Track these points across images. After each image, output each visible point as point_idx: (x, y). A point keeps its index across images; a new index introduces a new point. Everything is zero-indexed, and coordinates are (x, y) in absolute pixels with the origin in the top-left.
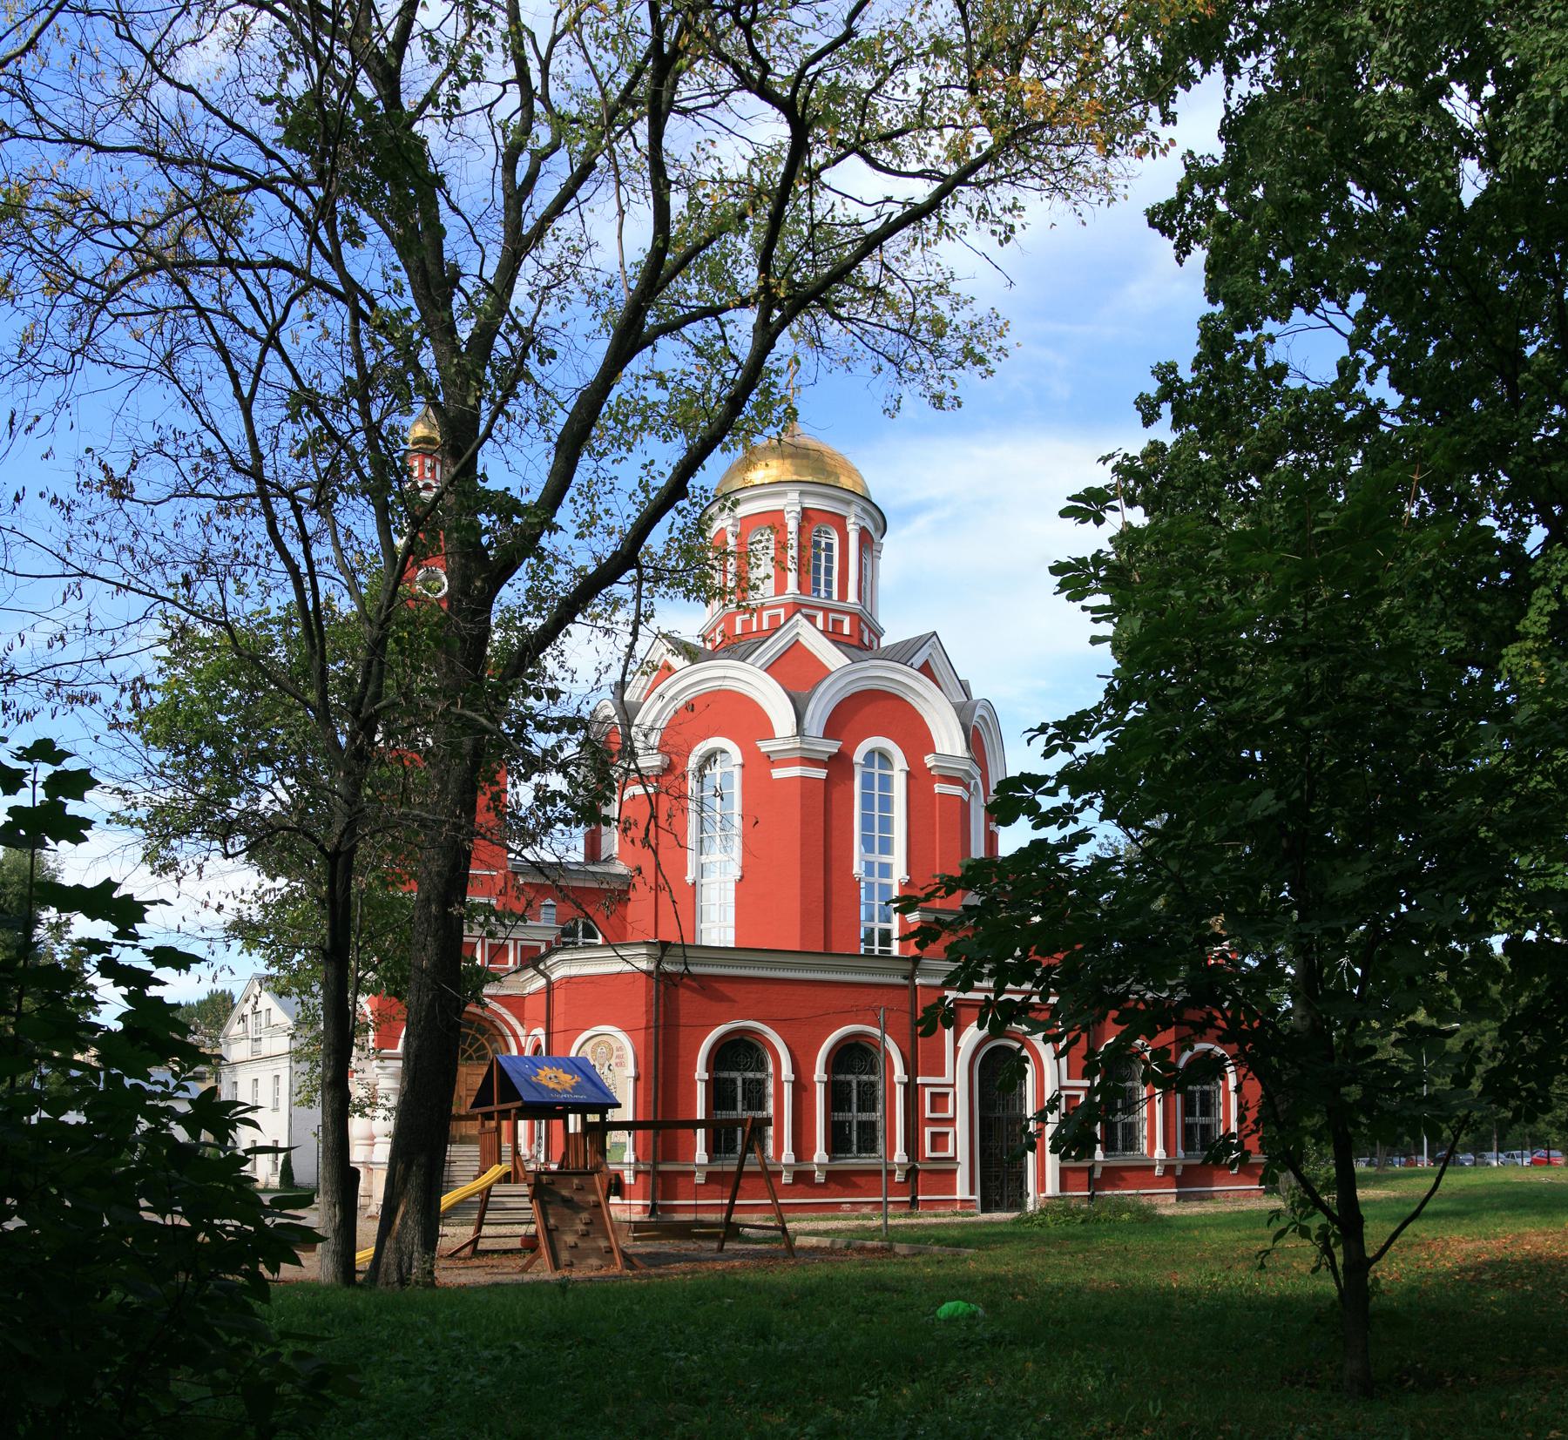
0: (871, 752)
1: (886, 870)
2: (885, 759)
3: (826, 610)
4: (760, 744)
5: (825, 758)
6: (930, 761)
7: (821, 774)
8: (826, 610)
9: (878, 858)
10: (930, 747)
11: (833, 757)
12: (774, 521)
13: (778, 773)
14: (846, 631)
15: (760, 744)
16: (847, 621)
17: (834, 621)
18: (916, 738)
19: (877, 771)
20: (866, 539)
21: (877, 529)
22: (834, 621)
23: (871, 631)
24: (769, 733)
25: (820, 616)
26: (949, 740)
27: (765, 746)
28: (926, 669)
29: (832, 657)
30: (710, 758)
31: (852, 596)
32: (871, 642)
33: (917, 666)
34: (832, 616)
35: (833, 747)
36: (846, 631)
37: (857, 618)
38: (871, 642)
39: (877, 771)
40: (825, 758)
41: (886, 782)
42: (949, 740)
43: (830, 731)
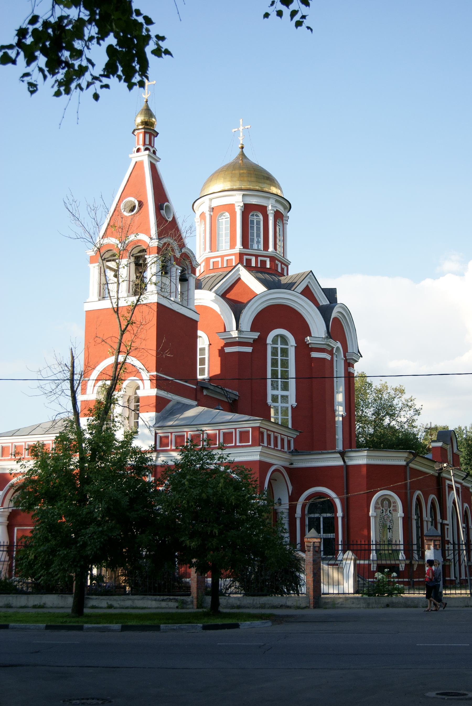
0: (277, 336)
1: (285, 398)
2: (284, 340)
3: (257, 256)
5: (251, 341)
7: (249, 349)
8: (257, 256)
9: (279, 393)
11: (255, 340)
12: (230, 208)
14: (268, 266)
17: (261, 261)
18: (300, 327)
19: (279, 346)
20: (278, 216)
21: (285, 208)
22: (261, 261)
23: (282, 263)
25: (253, 259)
26: (318, 328)
29: (258, 288)
31: (271, 249)
32: (282, 269)
33: (300, 291)
34: (259, 259)
35: (256, 335)
36: (268, 266)
37: (273, 259)
38: (282, 269)
39: (279, 346)
40: (251, 341)
41: (285, 352)
42: (318, 328)
43: (253, 329)
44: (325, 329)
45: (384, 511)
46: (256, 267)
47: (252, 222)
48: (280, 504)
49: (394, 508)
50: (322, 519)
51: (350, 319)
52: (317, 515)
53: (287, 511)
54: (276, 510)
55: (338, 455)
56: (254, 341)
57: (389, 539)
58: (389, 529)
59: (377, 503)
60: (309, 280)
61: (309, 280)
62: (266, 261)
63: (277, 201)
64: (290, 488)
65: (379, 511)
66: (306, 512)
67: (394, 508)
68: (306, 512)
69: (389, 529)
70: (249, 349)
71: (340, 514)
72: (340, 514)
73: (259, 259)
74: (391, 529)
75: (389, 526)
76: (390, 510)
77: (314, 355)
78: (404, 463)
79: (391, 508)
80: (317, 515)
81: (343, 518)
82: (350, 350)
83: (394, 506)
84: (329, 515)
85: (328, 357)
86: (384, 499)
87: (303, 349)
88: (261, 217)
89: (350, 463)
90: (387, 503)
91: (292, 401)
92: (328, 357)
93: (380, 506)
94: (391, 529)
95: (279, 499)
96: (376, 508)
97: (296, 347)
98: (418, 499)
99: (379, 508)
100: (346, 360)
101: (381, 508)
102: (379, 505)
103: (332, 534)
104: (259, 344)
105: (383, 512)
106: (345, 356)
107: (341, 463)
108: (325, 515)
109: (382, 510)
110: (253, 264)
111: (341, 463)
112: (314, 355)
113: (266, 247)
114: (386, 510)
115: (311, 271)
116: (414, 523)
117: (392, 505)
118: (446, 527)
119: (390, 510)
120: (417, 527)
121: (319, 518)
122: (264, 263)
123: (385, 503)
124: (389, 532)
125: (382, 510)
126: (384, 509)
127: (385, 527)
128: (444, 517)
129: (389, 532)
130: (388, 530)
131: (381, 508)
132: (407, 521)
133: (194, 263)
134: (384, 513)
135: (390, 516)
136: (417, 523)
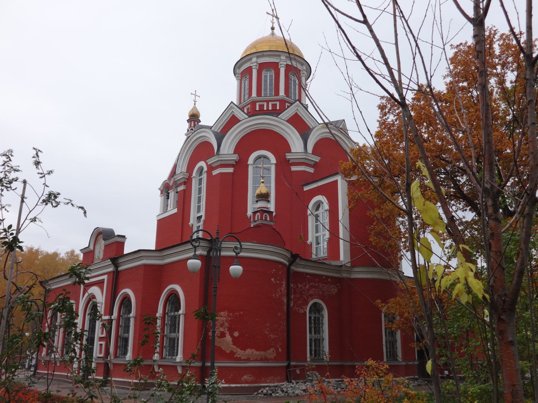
0: (259, 157)
6: (289, 156)
7: (231, 170)
8: (268, 102)
10: (289, 151)
12: (250, 69)
13: (215, 172)
14: (278, 108)
16: (278, 103)
20: (289, 68)
21: (302, 64)
25: (265, 104)
35: (235, 157)
36: (278, 108)
46: (268, 110)
47: (266, 77)
56: (236, 162)
70: (231, 170)
73: (270, 104)
77: (294, 168)
87: (283, 165)
88: (273, 73)
104: (241, 166)
110: (265, 109)
112: (294, 168)
113: (277, 93)
122: (274, 106)
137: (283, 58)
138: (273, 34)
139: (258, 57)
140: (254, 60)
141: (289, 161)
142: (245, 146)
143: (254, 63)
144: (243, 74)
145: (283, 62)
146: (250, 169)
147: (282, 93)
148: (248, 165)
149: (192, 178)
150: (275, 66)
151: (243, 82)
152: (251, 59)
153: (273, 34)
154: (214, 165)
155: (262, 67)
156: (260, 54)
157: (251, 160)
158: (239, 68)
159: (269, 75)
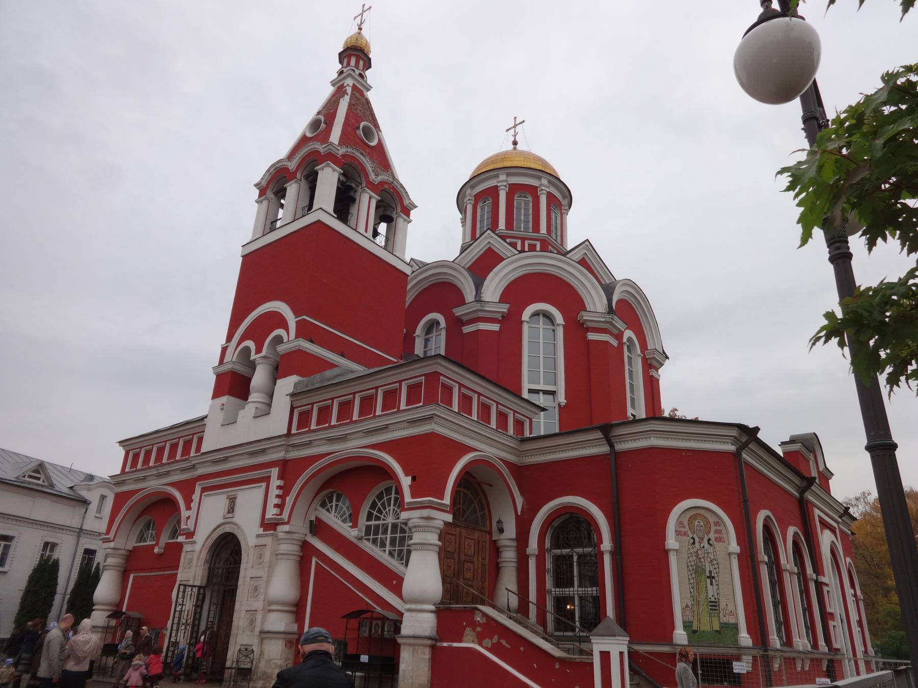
0: (536, 314)
3: (523, 240)
4: (454, 310)
5: (499, 316)
7: (495, 327)
8: (523, 240)
12: (493, 192)
13: (467, 329)
15: (454, 310)
20: (550, 197)
21: (564, 197)
24: (461, 301)
25: (519, 243)
26: (596, 303)
27: (459, 312)
28: (583, 262)
30: (432, 326)
35: (504, 308)
43: (503, 299)
44: (606, 302)
45: (697, 540)
48: (501, 531)
49: (717, 535)
50: (558, 552)
51: (644, 301)
52: (565, 551)
53: (515, 544)
54: (495, 541)
55: (599, 435)
56: (503, 317)
57: (713, 599)
58: (711, 577)
59: (680, 523)
60: (585, 251)
61: (585, 251)
62: (535, 245)
63: (549, 182)
64: (520, 501)
65: (687, 540)
66: (547, 545)
67: (717, 535)
68: (547, 545)
69: (711, 577)
70: (495, 327)
71: (607, 545)
72: (607, 545)
73: (527, 243)
74: (713, 578)
75: (710, 572)
76: (709, 540)
77: (592, 336)
78: (731, 448)
79: (712, 536)
80: (565, 551)
81: (613, 554)
82: (650, 346)
83: (716, 532)
84: (588, 550)
85: (614, 343)
86: (694, 514)
87: (576, 330)
88: (530, 199)
89: (620, 447)
90: (702, 523)
91: (562, 399)
92: (614, 343)
93: (687, 529)
94: (713, 578)
95: (499, 522)
96: (678, 533)
97: (564, 327)
98: (767, 528)
99: (685, 534)
100: (645, 360)
101: (689, 533)
102: (684, 527)
103: (594, 589)
104: (511, 323)
105: (694, 543)
106: (642, 352)
107: (606, 449)
108: (580, 550)
109: (693, 538)
111: (606, 449)
112: (592, 336)
113: (536, 228)
114: (702, 539)
115: (587, 240)
116: (764, 571)
117: (713, 528)
118: (825, 589)
119: (709, 540)
120: (772, 584)
121: (572, 556)
123: (696, 523)
124: (711, 584)
125: (693, 538)
126: (695, 536)
127: (701, 574)
128: (818, 568)
129: (711, 584)
130: (708, 580)
131: (691, 535)
132: (748, 560)
133: (406, 202)
134: (697, 544)
135: (711, 550)
136: (770, 574)
137: (544, 182)
138: (515, 148)
139: (508, 175)
140: (503, 177)
141: (583, 324)
142: (521, 291)
143: (503, 182)
144: (478, 197)
145: (543, 184)
146: (525, 328)
147: (543, 229)
148: (521, 322)
149: (414, 338)
150: (533, 191)
151: (479, 210)
152: (497, 176)
153: (515, 148)
154: (465, 318)
155: (513, 189)
156: (511, 170)
157: (526, 315)
158: (472, 187)
159: (523, 203)
